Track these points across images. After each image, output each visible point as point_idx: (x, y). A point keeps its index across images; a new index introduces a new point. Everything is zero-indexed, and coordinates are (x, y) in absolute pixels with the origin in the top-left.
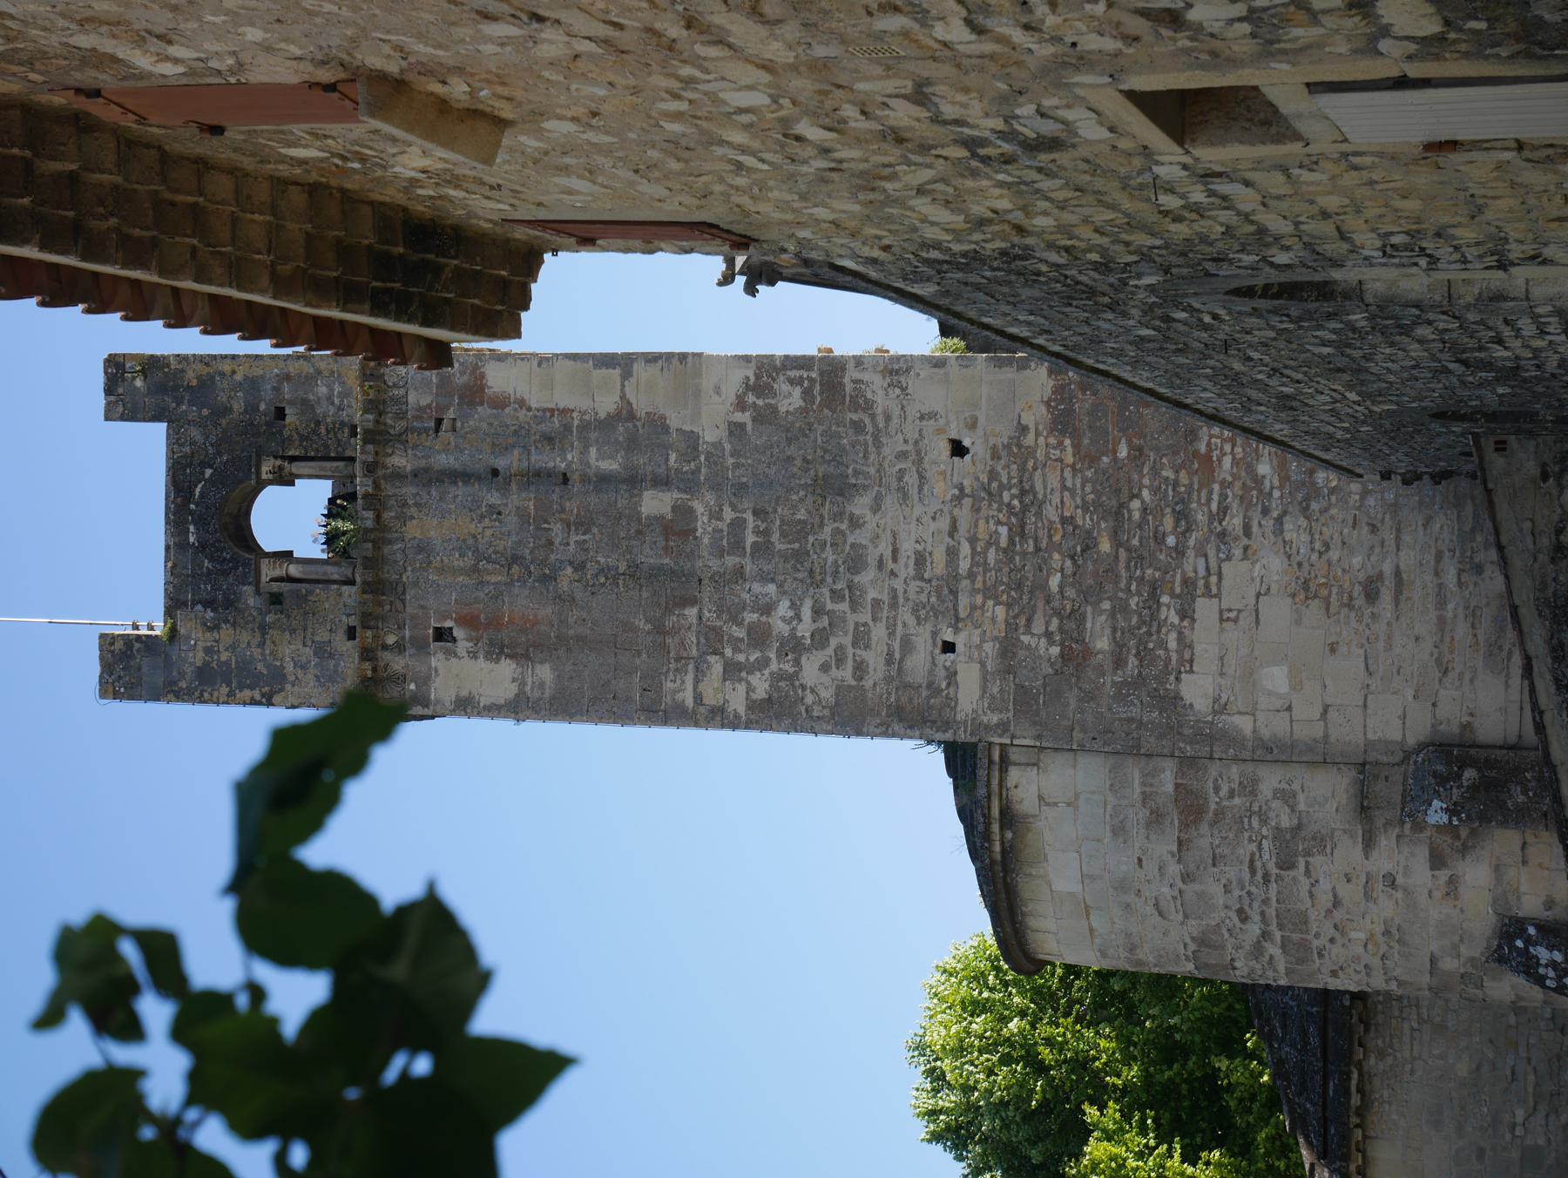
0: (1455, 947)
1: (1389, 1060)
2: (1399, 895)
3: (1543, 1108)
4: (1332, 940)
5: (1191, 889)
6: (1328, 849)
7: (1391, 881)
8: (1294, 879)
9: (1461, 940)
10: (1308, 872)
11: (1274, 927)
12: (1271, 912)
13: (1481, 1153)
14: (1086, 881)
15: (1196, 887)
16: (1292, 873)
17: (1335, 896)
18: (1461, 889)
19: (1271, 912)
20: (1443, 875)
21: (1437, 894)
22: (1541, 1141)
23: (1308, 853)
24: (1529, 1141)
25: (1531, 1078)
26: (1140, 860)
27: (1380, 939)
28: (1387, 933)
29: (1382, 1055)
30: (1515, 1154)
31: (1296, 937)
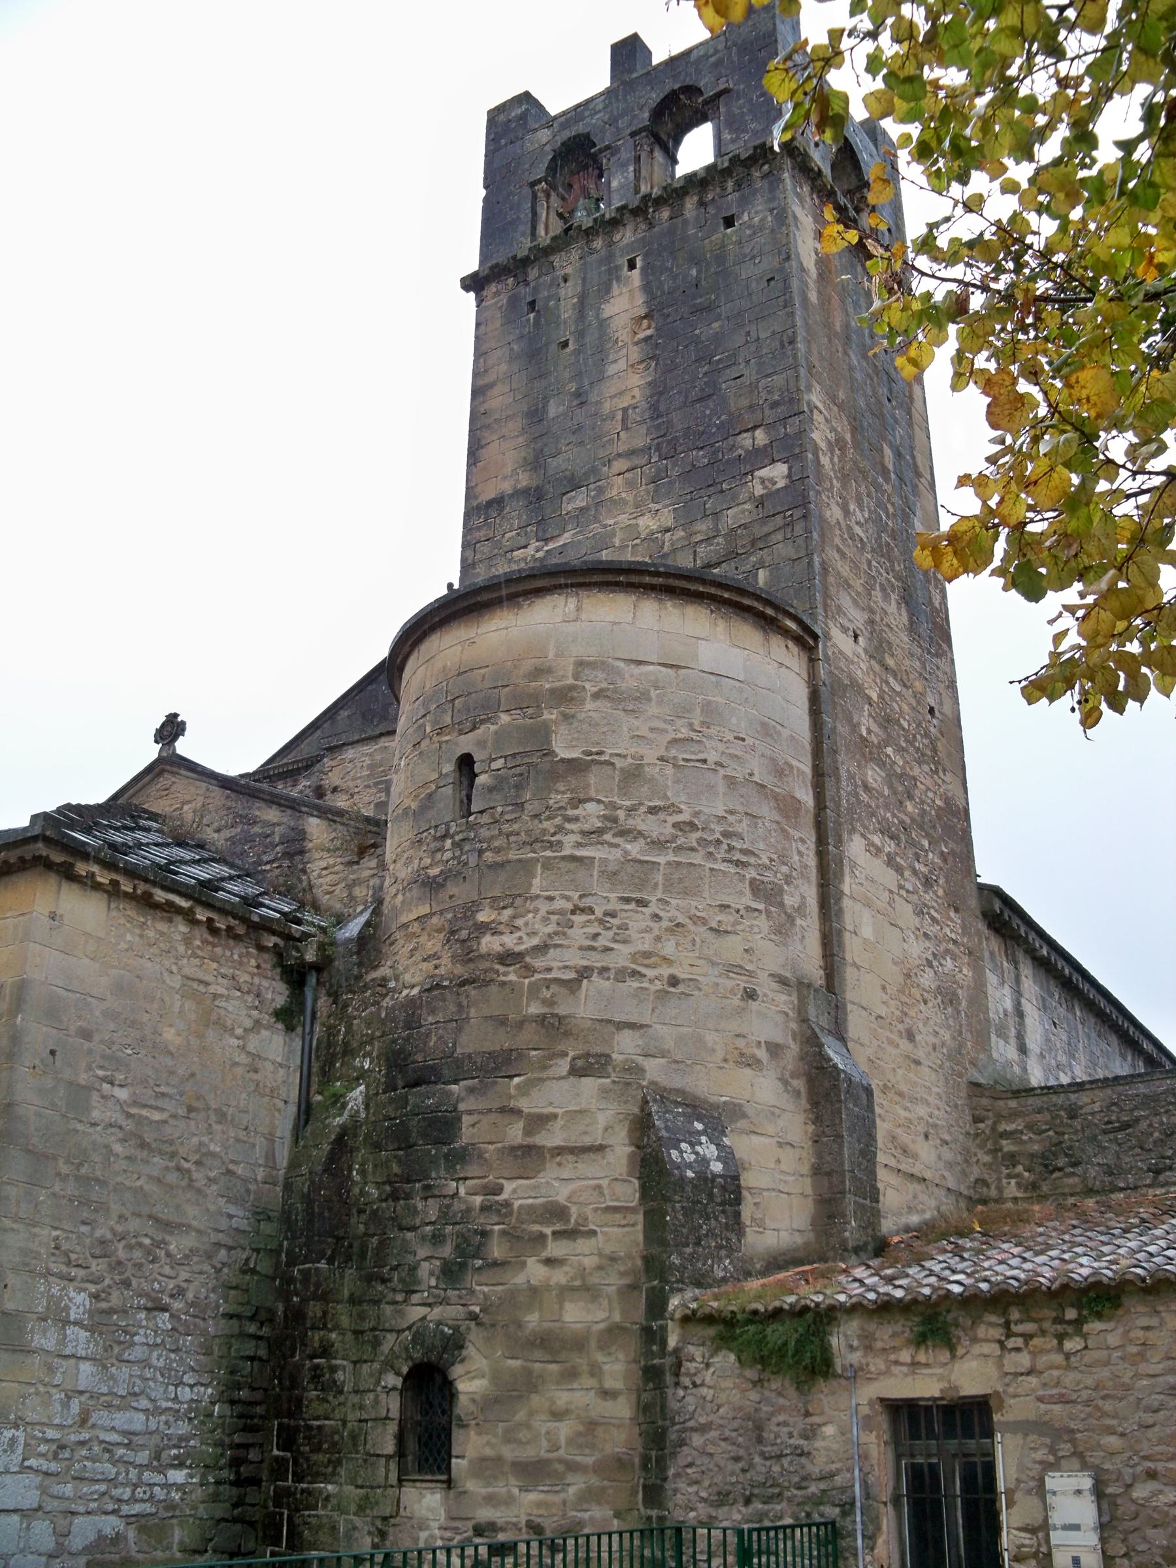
0: (663, 1054)
1: (181, 949)
2: (736, 1001)
3: (129, 1125)
4: (656, 917)
5: (718, 779)
6: (773, 937)
7: (750, 995)
8: (741, 893)
9: (676, 1062)
10: (748, 909)
11: (671, 857)
12: (697, 858)
13: (86, 1035)
14: (713, 678)
15: (721, 788)
16: (748, 892)
17: (726, 932)
18: (748, 1071)
19: (697, 858)
20: (762, 1054)
21: (741, 1043)
22: (96, 1114)
23: (768, 914)
24: (95, 1096)
25: (157, 1116)
26: (743, 740)
27: (666, 971)
28: (674, 981)
29: (187, 941)
30: (83, 1078)
31: (660, 878)
